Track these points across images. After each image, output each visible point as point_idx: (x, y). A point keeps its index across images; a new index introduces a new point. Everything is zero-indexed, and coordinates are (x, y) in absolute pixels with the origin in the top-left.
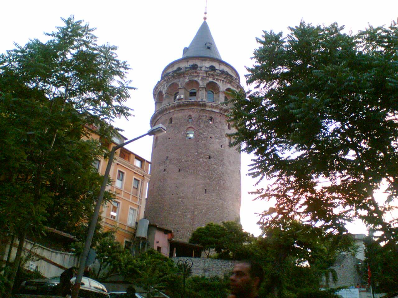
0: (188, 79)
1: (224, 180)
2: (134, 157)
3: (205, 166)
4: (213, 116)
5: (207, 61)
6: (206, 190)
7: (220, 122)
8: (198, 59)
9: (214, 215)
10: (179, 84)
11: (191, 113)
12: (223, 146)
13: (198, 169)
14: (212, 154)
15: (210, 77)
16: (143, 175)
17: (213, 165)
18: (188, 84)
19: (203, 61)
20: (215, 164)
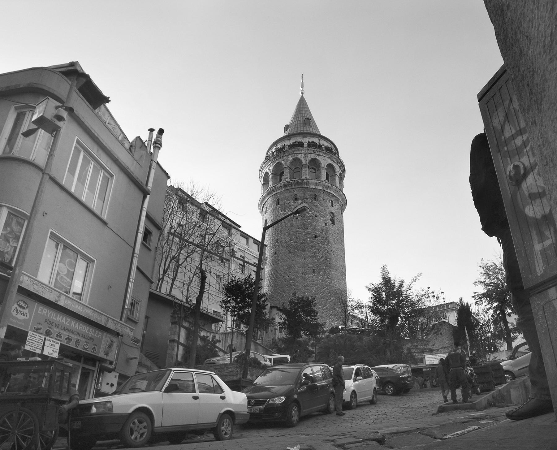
1: (330, 259)
6: (314, 270)
7: (323, 199)
8: (299, 136)
10: (283, 162)
11: (296, 192)
12: (327, 224)
14: (318, 233)
18: (292, 163)
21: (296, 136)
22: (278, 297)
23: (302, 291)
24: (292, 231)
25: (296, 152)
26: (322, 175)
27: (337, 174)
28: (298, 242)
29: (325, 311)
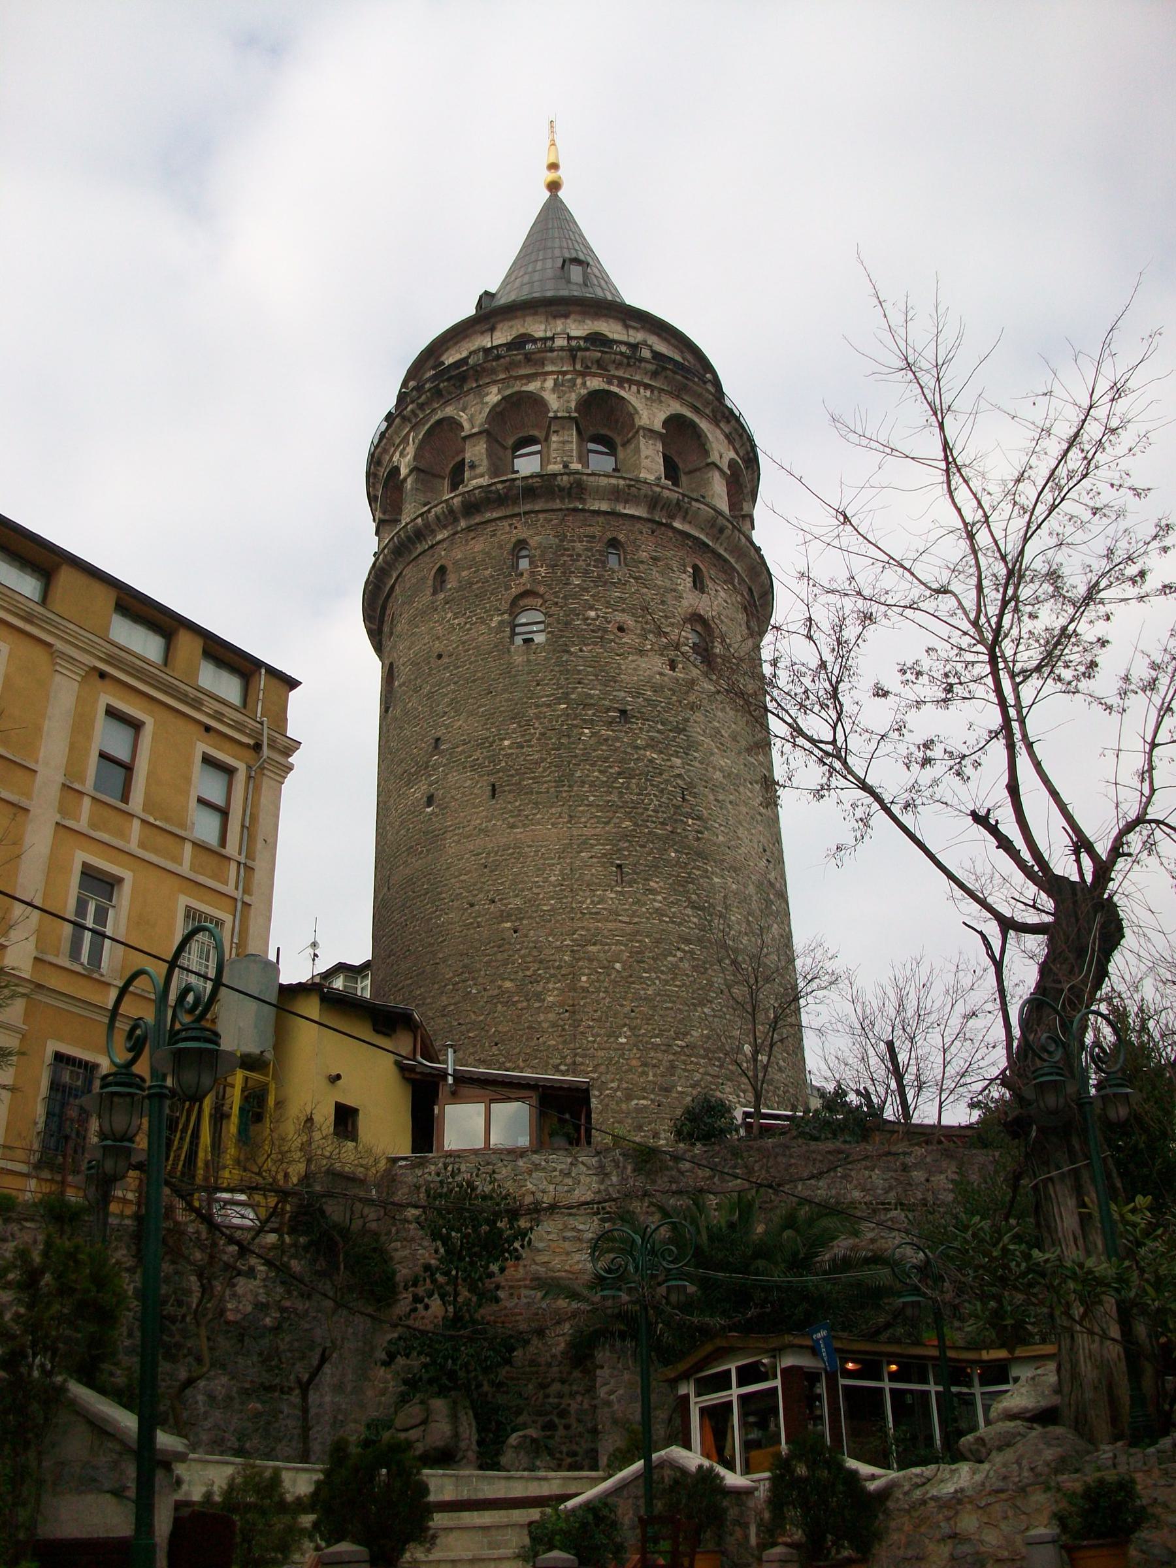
0: (499, 391)
1: (699, 818)
2: (199, 651)
3: (606, 759)
4: (621, 537)
5: (572, 316)
7: (655, 559)
8: (535, 314)
9: (666, 982)
10: (463, 418)
11: (521, 532)
13: (578, 774)
15: (594, 375)
16: (252, 742)
17: (642, 752)
18: (498, 415)
19: (555, 317)
20: (652, 745)
21: (519, 313)
22: (444, 1000)
23: (560, 967)
24: (506, 696)
25: (522, 372)
26: (645, 463)
27: (716, 457)
28: (534, 741)
29: (684, 1063)
